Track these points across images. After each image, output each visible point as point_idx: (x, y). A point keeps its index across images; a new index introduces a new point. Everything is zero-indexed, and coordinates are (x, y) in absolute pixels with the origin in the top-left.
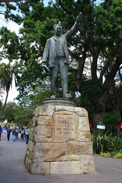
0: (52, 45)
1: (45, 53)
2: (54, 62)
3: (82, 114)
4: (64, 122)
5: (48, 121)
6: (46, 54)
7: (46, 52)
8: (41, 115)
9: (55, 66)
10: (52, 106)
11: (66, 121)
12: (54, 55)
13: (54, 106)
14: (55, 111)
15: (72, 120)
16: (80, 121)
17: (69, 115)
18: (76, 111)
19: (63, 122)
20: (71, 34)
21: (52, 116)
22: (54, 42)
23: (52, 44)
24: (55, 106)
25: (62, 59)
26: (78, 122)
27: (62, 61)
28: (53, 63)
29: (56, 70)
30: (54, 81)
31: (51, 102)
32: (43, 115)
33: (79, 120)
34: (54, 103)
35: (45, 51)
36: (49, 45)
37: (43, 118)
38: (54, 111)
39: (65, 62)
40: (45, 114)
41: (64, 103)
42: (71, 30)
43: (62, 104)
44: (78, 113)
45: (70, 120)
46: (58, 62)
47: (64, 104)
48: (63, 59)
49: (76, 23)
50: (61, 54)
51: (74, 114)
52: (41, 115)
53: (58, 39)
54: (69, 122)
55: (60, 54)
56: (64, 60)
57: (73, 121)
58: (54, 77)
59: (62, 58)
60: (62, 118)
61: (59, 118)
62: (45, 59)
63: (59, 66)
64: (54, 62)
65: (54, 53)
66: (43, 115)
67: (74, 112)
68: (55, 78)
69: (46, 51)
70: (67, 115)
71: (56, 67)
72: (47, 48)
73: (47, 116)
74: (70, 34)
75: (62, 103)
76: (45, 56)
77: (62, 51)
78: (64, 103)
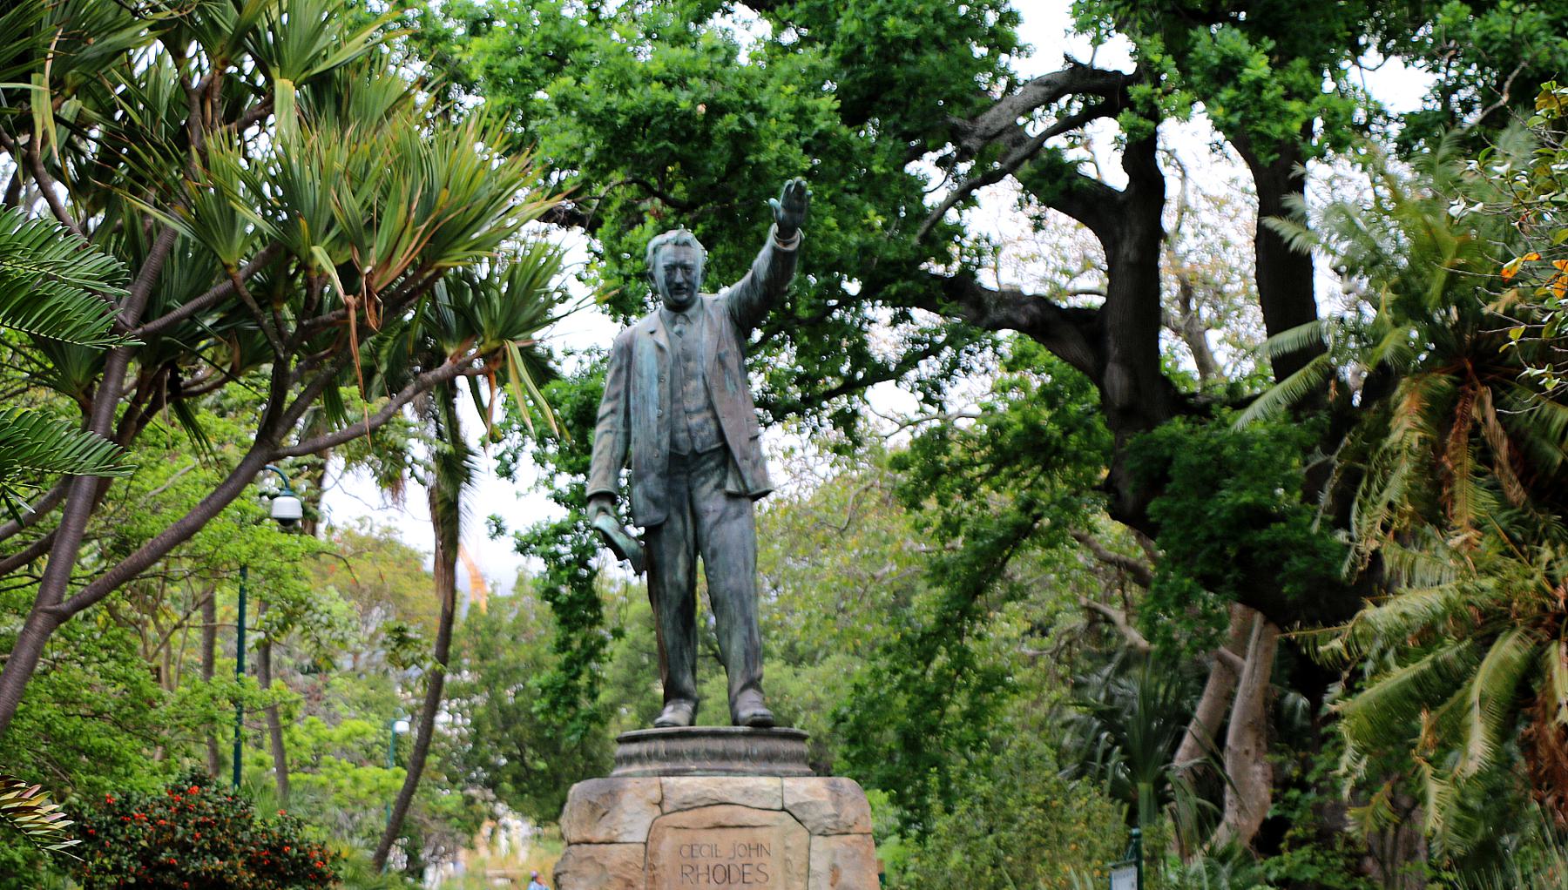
0: (641, 376)
1: (601, 436)
2: (661, 494)
3: (828, 822)
4: (720, 875)
5: (617, 877)
6: (608, 439)
7: (613, 425)
8: (578, 843)
9: (668, 519)
10: (646, 782)
11: (733, 871)
12: (658, 445)
13: (656, 780)
14: (663, 814)
15: (765, 859)
16: (820, 864)
17: (746, 830)
18: (789, 802)
19: (711, 871)
20: (756, 298)
21: (645, 844)
22: (653, 361)
23: (645, 374)
24: (664, 779)
25: (713, 470)
26: (804, 871)
27: (713, 481)
28: (655, 501)
29: (678, 542)
30: (673, 610)
31: (651, 757)
32: (589, 843)
33: (813, 855)
34: (662, 760)
35: (602, 419)
36: (624, 374)
37: (591, 858)
38: (657, 811)
39: (731, 486)
40: (601, 836)
41: (724, 756)
42: (753, 278)
43: (709, 765)
44: (807, 816)
45: (755, 860)
46: (684, 489)
47: (726, 765)
48: (718, 467)
49: (771, 240)
50: (705, 438)
51: (781, 820)
52: (578, 843)
53: (680, 333)
54: (747, 869)
55: (692, 439)
56: (725, 477)
57: (772, 865)
58: (668, 588)
59: (712, 464)
60: (705, 850)
61: (686, 850)
62: (602, 473)
63: (696, 518)
64: (661, 494)
65: (659, 433)
66: (589, 843)
67: (783, 809)
68: (675, 593)
69: (608, 420)
70: (737, 831)
71: (679, 526)
72: (617, 396)
73: (612, 843)
74: (751, 300)
75: (713, 755)
76: (607, 453)
77: (706, 421)
78: (724, 756)
